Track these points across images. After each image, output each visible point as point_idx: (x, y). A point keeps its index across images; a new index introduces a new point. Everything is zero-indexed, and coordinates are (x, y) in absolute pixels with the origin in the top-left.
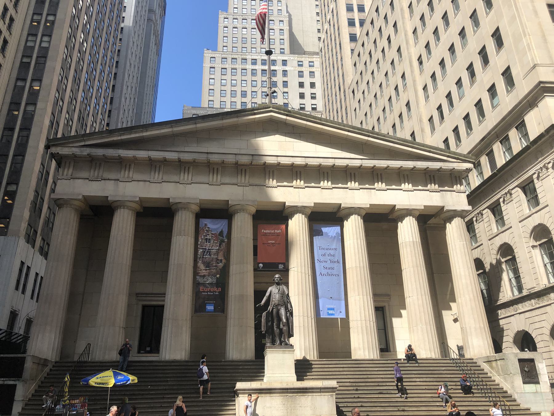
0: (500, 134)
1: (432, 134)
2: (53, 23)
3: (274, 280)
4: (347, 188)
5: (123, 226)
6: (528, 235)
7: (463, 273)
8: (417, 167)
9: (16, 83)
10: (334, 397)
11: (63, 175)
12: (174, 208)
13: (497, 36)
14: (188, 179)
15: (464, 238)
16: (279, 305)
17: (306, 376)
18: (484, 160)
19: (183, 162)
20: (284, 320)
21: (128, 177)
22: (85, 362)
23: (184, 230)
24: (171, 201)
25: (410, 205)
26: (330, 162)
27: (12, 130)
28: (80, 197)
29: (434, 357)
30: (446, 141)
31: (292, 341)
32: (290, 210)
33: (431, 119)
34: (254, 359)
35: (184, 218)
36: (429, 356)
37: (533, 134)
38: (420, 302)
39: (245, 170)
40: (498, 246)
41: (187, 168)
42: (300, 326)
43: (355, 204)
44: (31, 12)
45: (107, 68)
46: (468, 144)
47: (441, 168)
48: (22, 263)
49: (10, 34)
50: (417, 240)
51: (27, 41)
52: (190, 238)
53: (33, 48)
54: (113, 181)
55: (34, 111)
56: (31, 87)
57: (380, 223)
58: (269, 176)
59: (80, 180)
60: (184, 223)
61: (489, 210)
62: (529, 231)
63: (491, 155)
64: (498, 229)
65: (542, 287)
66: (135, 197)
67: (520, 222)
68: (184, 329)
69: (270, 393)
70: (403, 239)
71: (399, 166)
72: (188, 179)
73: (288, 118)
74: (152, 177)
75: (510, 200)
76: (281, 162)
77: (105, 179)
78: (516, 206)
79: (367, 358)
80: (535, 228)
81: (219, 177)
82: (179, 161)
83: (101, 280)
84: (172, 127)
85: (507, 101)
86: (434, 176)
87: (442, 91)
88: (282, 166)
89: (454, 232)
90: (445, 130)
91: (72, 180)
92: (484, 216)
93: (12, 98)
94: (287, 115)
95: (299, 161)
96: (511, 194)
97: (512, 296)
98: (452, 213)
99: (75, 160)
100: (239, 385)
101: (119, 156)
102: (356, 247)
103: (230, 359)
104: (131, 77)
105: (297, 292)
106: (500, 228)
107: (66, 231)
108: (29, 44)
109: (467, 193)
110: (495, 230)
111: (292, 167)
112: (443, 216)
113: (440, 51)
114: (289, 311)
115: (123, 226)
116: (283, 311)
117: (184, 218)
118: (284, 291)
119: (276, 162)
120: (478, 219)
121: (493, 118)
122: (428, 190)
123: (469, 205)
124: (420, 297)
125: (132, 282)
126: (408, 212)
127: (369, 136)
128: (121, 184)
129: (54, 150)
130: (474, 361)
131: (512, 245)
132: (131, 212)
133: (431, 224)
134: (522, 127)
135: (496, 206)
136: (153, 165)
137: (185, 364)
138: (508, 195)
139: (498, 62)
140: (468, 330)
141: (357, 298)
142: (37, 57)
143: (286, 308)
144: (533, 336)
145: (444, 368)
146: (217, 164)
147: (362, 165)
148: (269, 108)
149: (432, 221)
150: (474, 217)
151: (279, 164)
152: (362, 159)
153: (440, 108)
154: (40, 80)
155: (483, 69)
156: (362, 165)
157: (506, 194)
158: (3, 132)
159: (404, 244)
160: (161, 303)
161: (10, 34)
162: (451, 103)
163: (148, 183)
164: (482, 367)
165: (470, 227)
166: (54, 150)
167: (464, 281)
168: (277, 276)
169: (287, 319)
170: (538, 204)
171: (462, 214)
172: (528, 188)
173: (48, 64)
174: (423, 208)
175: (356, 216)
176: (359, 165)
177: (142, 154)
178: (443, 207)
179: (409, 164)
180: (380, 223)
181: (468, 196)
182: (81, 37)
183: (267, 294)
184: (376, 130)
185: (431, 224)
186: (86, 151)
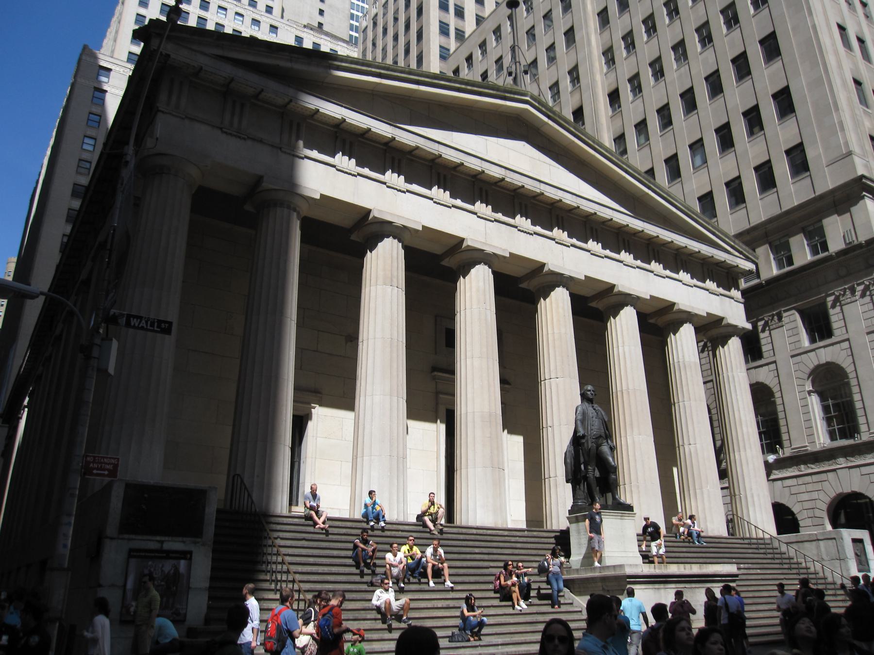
6: (806, 376)
7: (743, 418)
16: (601, 436)
62: (808, 371)
65: (818, 448)
73: (550, 122)
77: (254, 139)
94: (549, 117)
98: (730, 330)
103: (464, 524)
123: (748, 319)
126: (688, 317)
127: (649, 188)
138: (776, 317)
144: (795, 510)
148: (525, 95)
159: (681, 364)
167: (745, 429)
178: (722, 319)
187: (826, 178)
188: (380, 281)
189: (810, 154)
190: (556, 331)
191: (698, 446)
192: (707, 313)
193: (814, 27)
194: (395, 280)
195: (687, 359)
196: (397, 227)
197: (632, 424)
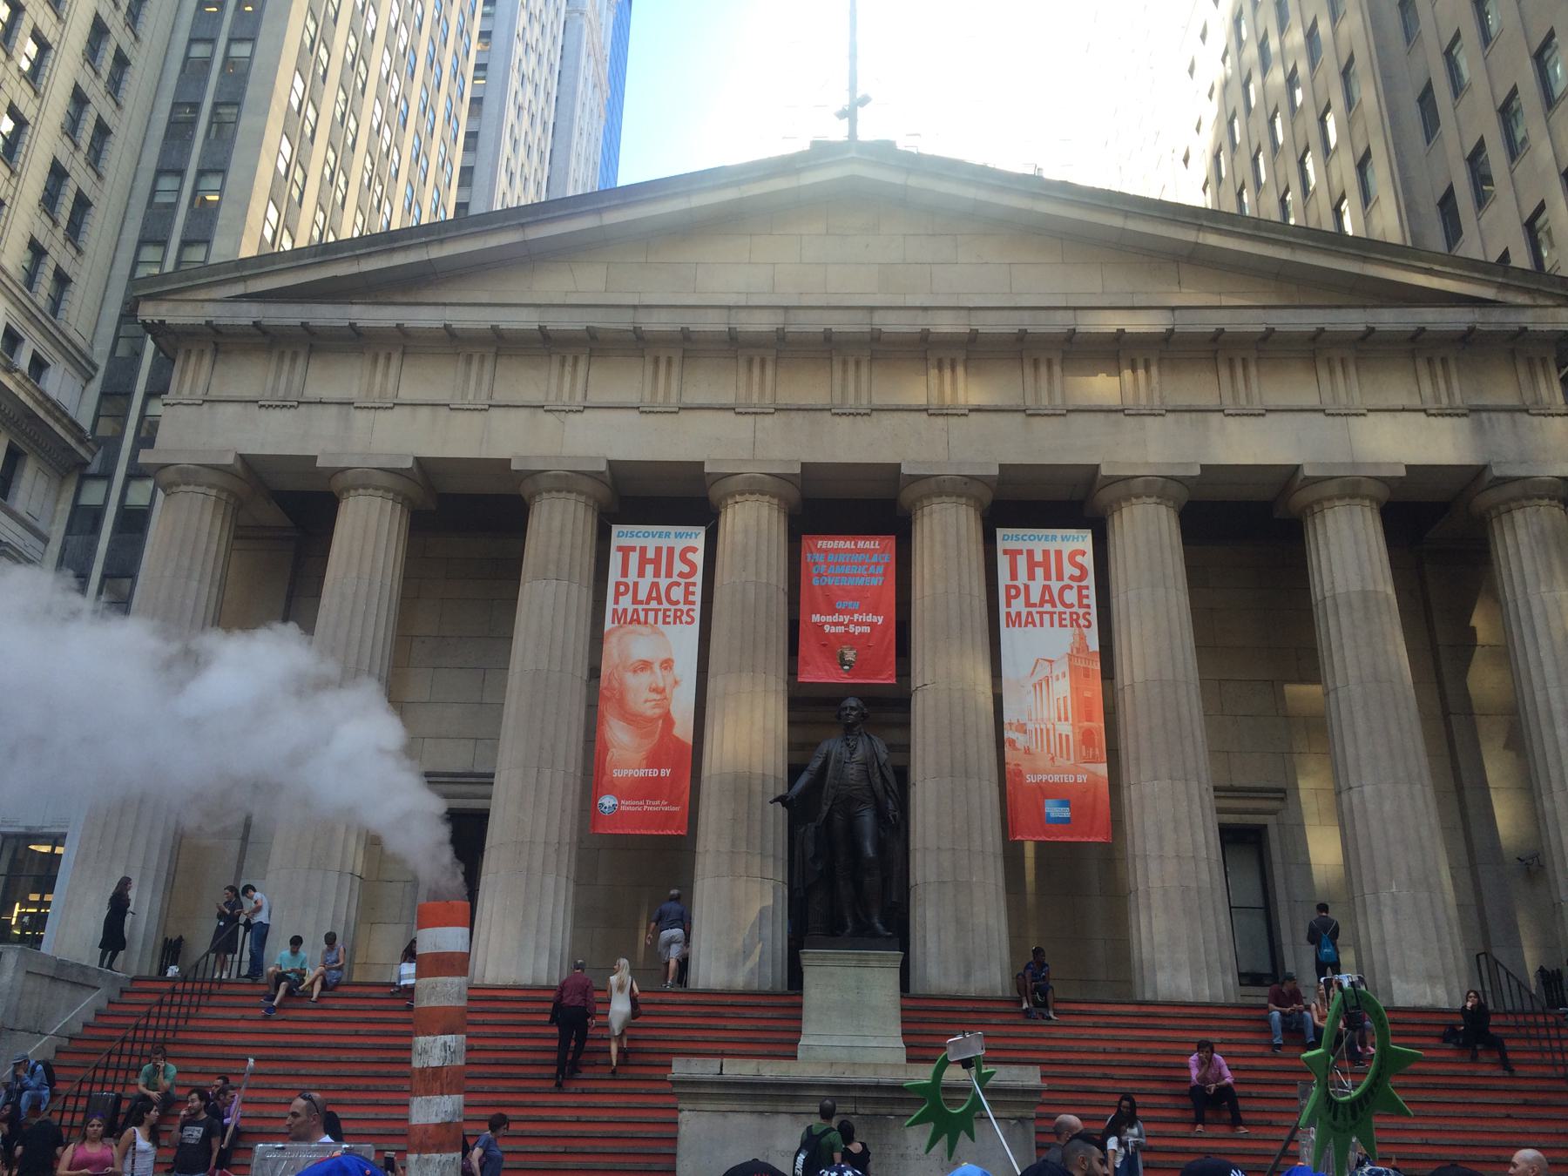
8: (1379, 327)
9: (155, 182)
10: (1032, 1127)
12: (526, 489)
20: (869, 850)
24: (514, 466)
25: (1354, 465)
41: (570, 360)
43: (1147, 464)
45: (436, 150)
52: (575, 587)
54: (334, 409)
56: (195, 191)
57: (1245, 535)
69: (793, 1099)
70: (1326, 587)
76: (885, 329)
79: (1190, 998)
91: (206, 406)
93: (144, 228)
95: (945, 325)
100: (681, 1068)
101: (352, 326)
116: (867, 819)
117: (556, 524)
119: (867, 329)
128: (360, 418)
142: (216, 105)
143: (881, 814)
154: (222, 171)
156: (1171, 332)
158: (118, 330)
159: (1329, 602)
161: (136, 37)
163: (444, 411)
169: (881, 846)
173: (245, 122)
174: (1402, 472)
179: (1354, 320)
186: (248, 314)
190: (928, 591)
191: (1368, 789)
192: (1409, 468)
194: (552, 567)
195: (1340, 590)
196: (557, 476)
197: (1138, 759)
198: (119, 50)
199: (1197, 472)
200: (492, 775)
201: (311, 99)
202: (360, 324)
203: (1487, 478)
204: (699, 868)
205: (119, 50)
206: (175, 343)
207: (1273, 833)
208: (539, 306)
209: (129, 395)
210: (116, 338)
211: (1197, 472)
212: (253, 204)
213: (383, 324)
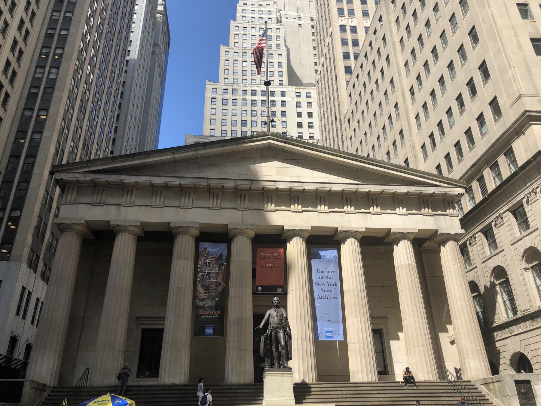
0: (489, 160)
1: (425, 160)
2: (61, 55)
3: (272, 303)
4: (344, 212)
5: (124, 250)
6: (520, 258)
7: (458, 296)
11: (66, 200)
12: (174, 232)
13: (483, 68)
14: (188, 204)
15: (458, 261)
16: (277, 327)
17: (305, 399)
18: (475, 185)
19: (184, 187)
20: (283, 343)
21: (130, 202)
22: (84, 387)
23: (184, 254)
25: (405, 229)
26: (326, 187)
27: (18, 157)
28: (83, 222)
29: (432, 379)
30: (438, 167)
31: (291, 363)
32: (289, 233)
33: (423, 147)
34: (253, 383)
35: (184, 242)
36: (427, 379)
37: (521, 160)
38: (417, 324)
39: (245, 195)
40: (492, 268)
41: (188, 193)
42: (298, 350)
44: (40, 46)
46: (459, 170)
47: (434, 193)
48: (24, 288)
49: (19, 65)
50: (413, 263)
51: (35, 72)
52: (189, 262)
53: (41, 79)
54: (115, 207)
55: (40, 139)
56: (38, 116)
57: (377, 247)
58: (295, 201)
59: (83, 205)
60: (184, 246)
61: (481, 234)
62: (521, 254)
63: (481, 180)
64: (491, 252)
66: (137, 221)
67: (512, 245)
68: (183, 352)
71: (394, 191)
72: (188, 204)
73: (286, 145)
74: (182, 203)
75: (502, 223)
76: (279, 187)
78: (507, 229)
80: (526, 251)
81: (219, 201)
82: (180, 186)
83: (102, 305)
84: (173, 154)
85: (495, 130)
86: (427, 201)
87: (434, 119)
88: (280, 191)
89: (448, 254)
90: (437, 157)
91: (75, 205)
92: (477, 239)
93: (19, 127)
94: (285, 143)
95: (297, 186)
96: (502, 218)
97: (507, 318)
98: (446, 236)
99: (78, 186)
101: (122, 182)
102: (353, 269)
103: (229, 382)
104: (135, 106)
105: (295, 315)
106: (492, 251)
107: (68, 255)
108: (38, 75)
109: (460, 217)
110: (488, 253)
111: (290, 192)
112: (437, 239)
113: (430, 82)
114: (287, 334)
115: (124, 250)
116: (281, 334)
118: (282, 314)
119: (274, 187)
120: (471, 242)
121: (482, 145)
122: (422, 214)
124: (416, 318)
125: (132, 305)
126: (403, 236)
127: (364, 162)
129: (58, 176)
130: (472, 383)
131: (505, 267)
132: (132, 237)
133: (426, 247)
134: (509, 153)
135: (488, 230)
136: (154, 190)
137: (184, 388)
139: (485, 92)
140: (465, 353)
141: (355, 320)
142: (45, 88)
145: (442, 391)
146: (217, 189)
147: (357, 190)
149: (427, 244)
150: (467, 240)
151: (277, 189)
152: (357, 184)
153: (432, 136)
154: (47, 110)
155: (471, 99)
156: (357, 190)
157: (497, 217)
158: (9, 160)
160: (161, 327)
161: (19, 65)
162: (442, 132)
163: (149, 208)
164: (479, 390)
165: (464, 250)
166: (58, 176)
167: (459, 303)
168: (275, 299)
170: (528, 227)
171: (455, 238)
172: (519, 213)
174: (417, 231)
175: (353, 239)
176: (354, 190)
177: (144, 180)
178: (437, 230)
179: (403, 189)
180: (377, 247)
181: (461, 220)
182: (88, 69)
183: (266, 317)
184: (371, 156)
185: (426, 247)
187: (510, 116)
188: (175, 258)
189: (500, 104)
193: (492, 15)
194: (183, 255)
198: (14, 70)
199: (364, 230)
200: (164, 318)
201: (77, 87)
202: (124, 181)
203: (439, 233)
204: (228, 347)
205: (14, 70)
206: (64, 186)
207: (384, 331)
208: (179, 177)
209: (12, 182)
210: (9, 163)
211: (364, 230)
212: (58, 121)
213: (131, 181)
